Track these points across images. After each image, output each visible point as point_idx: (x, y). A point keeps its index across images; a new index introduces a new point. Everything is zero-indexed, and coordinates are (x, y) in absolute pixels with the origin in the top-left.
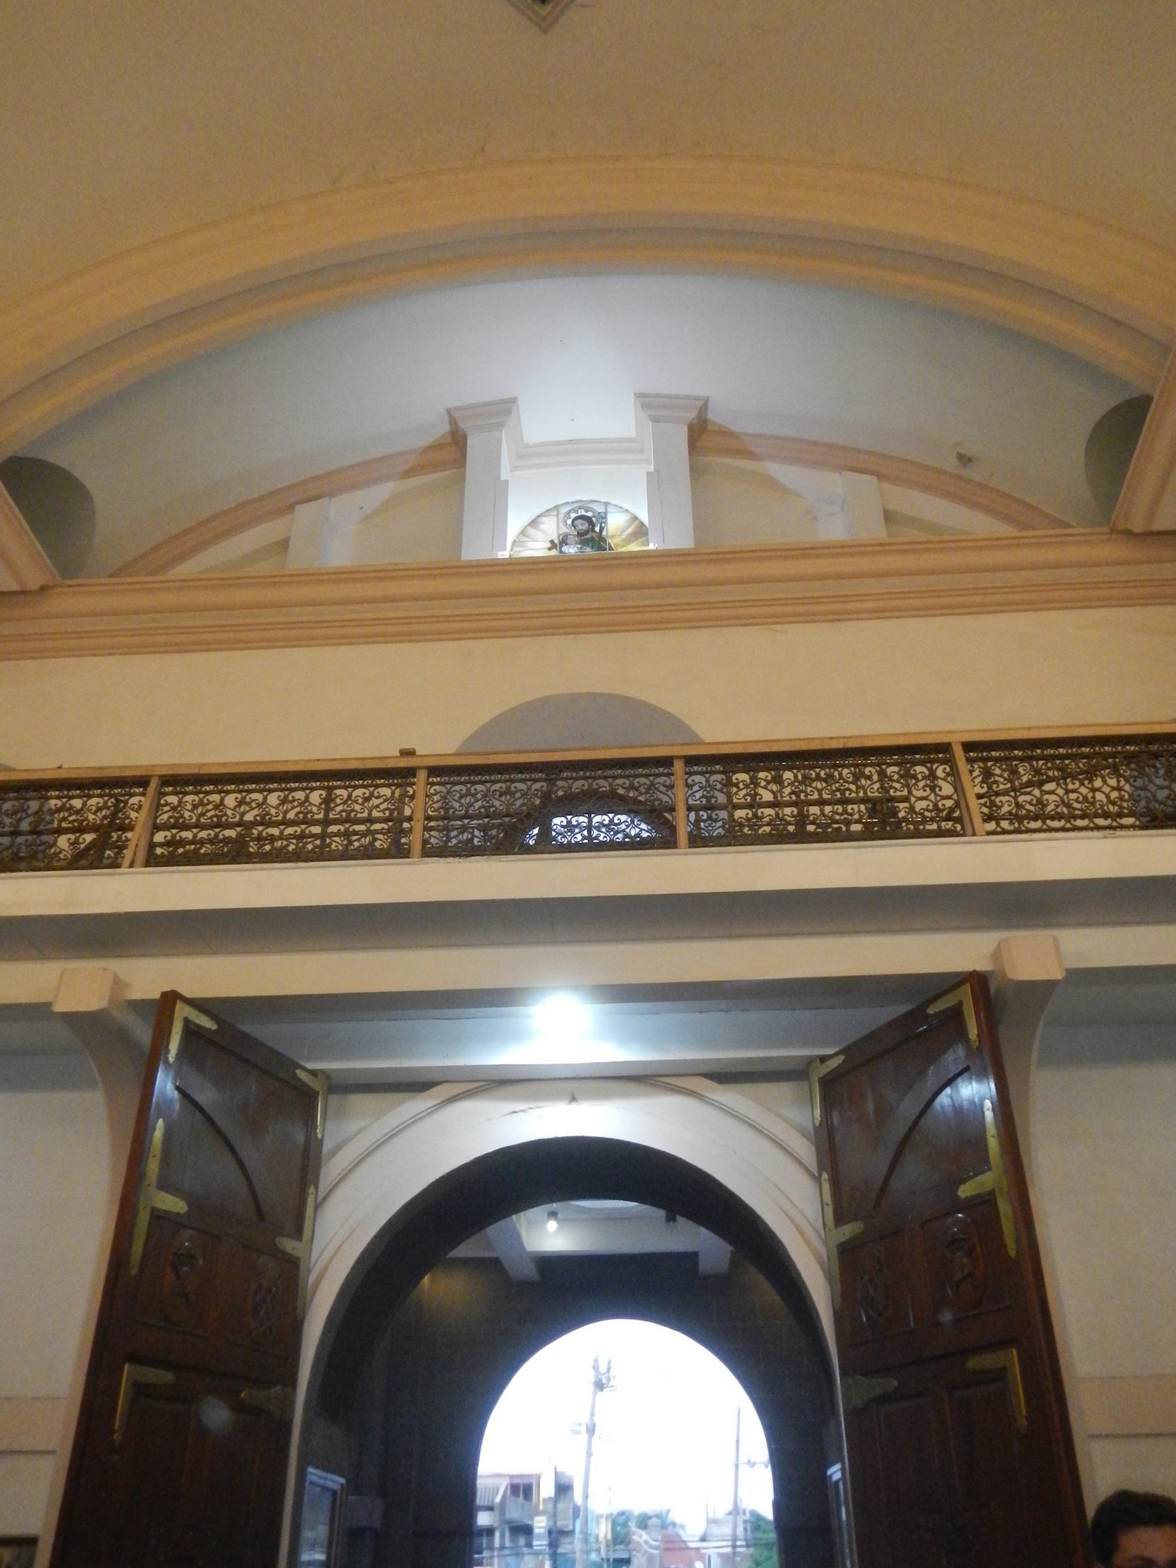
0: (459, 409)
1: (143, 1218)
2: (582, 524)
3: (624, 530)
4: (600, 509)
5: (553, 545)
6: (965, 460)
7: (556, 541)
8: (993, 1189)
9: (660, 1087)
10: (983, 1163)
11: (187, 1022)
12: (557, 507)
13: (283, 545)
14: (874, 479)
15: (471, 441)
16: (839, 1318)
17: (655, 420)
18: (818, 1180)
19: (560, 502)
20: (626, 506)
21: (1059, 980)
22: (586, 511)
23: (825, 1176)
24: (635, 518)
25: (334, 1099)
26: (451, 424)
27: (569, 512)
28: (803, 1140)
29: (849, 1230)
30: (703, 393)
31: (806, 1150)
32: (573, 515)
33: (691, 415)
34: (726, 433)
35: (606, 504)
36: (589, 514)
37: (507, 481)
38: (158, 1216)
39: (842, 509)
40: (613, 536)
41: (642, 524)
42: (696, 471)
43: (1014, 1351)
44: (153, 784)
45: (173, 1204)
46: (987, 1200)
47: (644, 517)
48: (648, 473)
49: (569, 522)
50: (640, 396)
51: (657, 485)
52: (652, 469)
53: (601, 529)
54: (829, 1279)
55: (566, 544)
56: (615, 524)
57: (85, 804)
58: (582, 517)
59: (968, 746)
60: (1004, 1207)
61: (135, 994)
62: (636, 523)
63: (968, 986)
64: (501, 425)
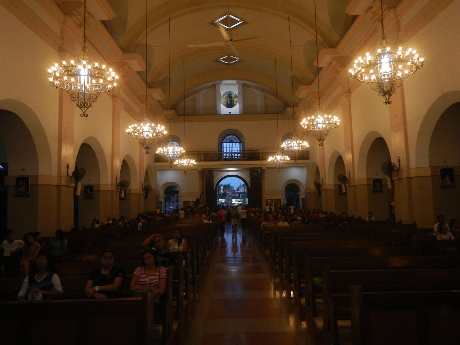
4: (232, 93)
12: (226, 92)
13: (195, 98)
15: (217, 87)
17: (238, 84)
18: (250, 177)
20: (235, 92)
24: (236, 94)
27: (228, 93)
31: (249, 175)
33: (243, 84)
35: (232, 92)
41: (236, 95)
42: (243, 89)
48: (238, 93)
56: (233, 95)
61: (202, 168)
64: (220, 84)
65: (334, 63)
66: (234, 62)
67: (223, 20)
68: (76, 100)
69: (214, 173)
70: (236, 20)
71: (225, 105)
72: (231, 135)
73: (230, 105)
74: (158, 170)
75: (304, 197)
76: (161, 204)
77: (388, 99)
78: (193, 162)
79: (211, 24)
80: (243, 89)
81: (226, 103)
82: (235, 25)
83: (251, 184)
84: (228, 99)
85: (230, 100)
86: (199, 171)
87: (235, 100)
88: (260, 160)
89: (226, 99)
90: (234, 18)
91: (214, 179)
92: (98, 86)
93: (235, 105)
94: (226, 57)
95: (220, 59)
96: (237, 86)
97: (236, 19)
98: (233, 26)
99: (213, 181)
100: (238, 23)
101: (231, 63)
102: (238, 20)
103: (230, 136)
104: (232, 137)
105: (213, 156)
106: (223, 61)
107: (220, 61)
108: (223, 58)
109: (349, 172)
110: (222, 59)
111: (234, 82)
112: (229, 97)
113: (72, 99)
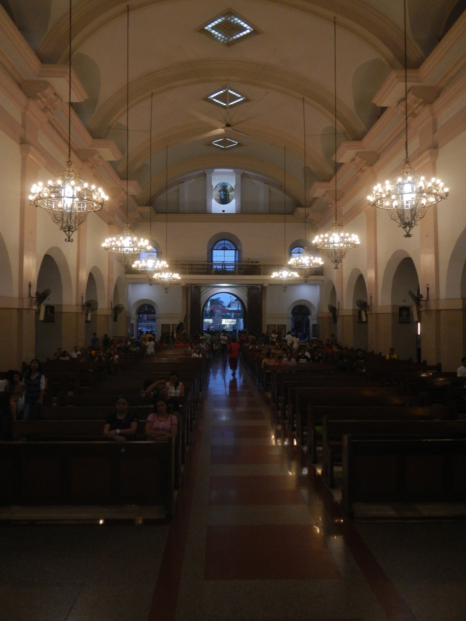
4: (226, 184)
12: (220, 183)
13: (178, 190)
15: (207, 175)
16: (248, 309)
17: (236, 174)
20: (230, 184)
24: (232, 187)
31: (246, 294)
32: (222, 185)
35: (227, 183)
36: (225, 185)
40: (228, 190)
47: (234, 187)
49: (222, 187)
52: (235, 184)
56: (229, 187)
58: (223, 186)
64: (212, 173)
65: (358, 160)
66: (231, 146)
67: (219, 95)
68: (59, 222)
69: (202, 290)
70: (236, 96)
71: (218, 200)
72: (224, 240)
73: (224, 200)
75: (315, 322)
77: (409, 231)
78: (177, 276)
79: (204, 100)
80: (241, 180)
81: (219, 198)
82: (234, 102)
83: (249, 305)
84: (222, 192)
85: (224, 194)
86: (182, 286)
87: (231, 194)
89: (219, 193)
90: (234, 93)
92: (82, 204)
94: (221, 139)
95: (213, 142)
96: (234, 176)
97: (237, 95)
98: (232, 103)
99: (200, 300)
100: (239, 100)
101: (227, 147)
102: (239, 96)
103: (224, 241)
104: (225, 243)
105: (201, 268)
106: (217, 145)
107: (213, 144)
108: (217, 141)
109: (371, 297)
110: (215, 142)
111: (231, 171)
113: (55, 221)
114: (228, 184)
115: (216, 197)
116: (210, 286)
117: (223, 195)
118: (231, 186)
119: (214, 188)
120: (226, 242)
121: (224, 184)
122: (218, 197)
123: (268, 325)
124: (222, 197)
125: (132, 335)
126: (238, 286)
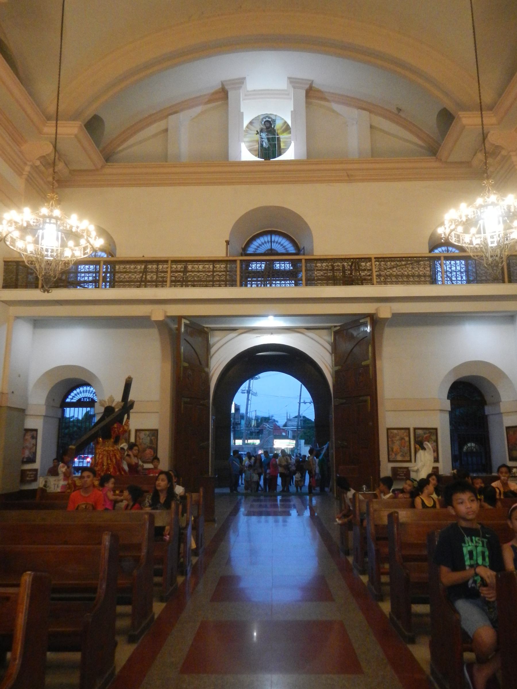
0: (226, 81)
1: (182, 368)
2: (268, 124)
3: (282, 127)
4: (273, 118)
5: (258, 133)
6: (399, 110)
7: (259, 131)
8: (369, 364)
9: (293, 331)
10: (368, 359)
11: (184, 322)
12: (258, 116)
13: (166, 130)
14: (368, 113)
16: (334, 386)
17: (294, 87)
18: (331, 354)
19: (260, 114)
20: (283, 117)
21: (389, 318)
22: (269, 118)
23: (333, 354)
24: (285, 122)
25: (211, 332)
26: (222, 86)
27: (263, 119)
28: (328, 345)
29: (337, 368)
30: (311, 78)
31: (329, 348)
32: (264, 120)
33: (307, 86)
34: (319, 91)
35: (276, 116)
36: (270, 120)
37: (243, 113)
38: (185, 368)
39: (357, 123)
40: (278, 130)
41: (288, 125)
42: (308, 104)
43: (369, 397)
44: (170, 262)
45: (186, 365)
46: (368, 366)
47: (289, 122)
48: (292, 112)
49: (263, 123)
50: (289, 78)
51: (294, 114)
52: (292, 110)
53: (274, 126)
54: (332, 377)
55: (262, 132)
56: (278, 125)
57: (152, 267)
58: (267, 121)
59: (375, 258)
60: (371, 368)
61: (169, 314)
62: (286, 125)
63: (369, 318)
64: (239, 88)
69: (212, 340)
71: (255, 150)
72: (271, 233)
74: (17, 318)
76: (35, 438)
80: (307, 107)
81: (257, 146)
83: (337, 375)
84: (264, 135)
85: (268, 139)
87: (283, 137)
88: (373, 284)
89: (258, 136)
91: (211, 358)
93: (284, 152)
96: (291, 99)
99: (207, 365)
104: (273, 240)
112: (267, 128)
114: (277, 118)
115: (251, 144)
116: (234, 330)
117: (266, 141)
118: (283, 122)
119: (247, 127)
120: (275, 238)
121: (267, 117)
122: (255, 144)
123: (388, 429)
124: (264, 144)
125: (32, 460)
126: (308, 329)
